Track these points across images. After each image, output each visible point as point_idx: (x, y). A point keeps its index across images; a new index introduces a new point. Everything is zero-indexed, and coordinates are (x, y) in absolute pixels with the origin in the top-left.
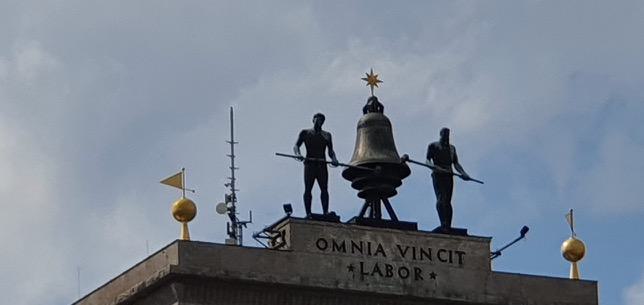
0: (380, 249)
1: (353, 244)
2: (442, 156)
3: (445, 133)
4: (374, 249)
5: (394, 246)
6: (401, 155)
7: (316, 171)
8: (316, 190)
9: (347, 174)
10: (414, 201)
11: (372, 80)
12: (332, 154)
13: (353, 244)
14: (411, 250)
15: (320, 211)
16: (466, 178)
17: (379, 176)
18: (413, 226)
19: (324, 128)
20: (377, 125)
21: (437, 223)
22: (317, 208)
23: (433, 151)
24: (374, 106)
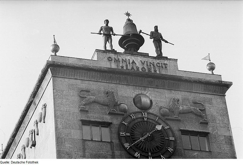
0: (133, 62)
1: (122, 59)
3: (156, 28)
4: (131, 62)
5: (139, 61)
6: (138, 30)
8: (108, 45)
12: (112, 32)
13: (122, 59)
14: (146, 62)
15: (110, 49)
16: (166, 42)
18: (146, 55)
19: (109, 25)
20: (130, 24)
21: (155, 55)
22: (109, 48)
24: (129, 20)
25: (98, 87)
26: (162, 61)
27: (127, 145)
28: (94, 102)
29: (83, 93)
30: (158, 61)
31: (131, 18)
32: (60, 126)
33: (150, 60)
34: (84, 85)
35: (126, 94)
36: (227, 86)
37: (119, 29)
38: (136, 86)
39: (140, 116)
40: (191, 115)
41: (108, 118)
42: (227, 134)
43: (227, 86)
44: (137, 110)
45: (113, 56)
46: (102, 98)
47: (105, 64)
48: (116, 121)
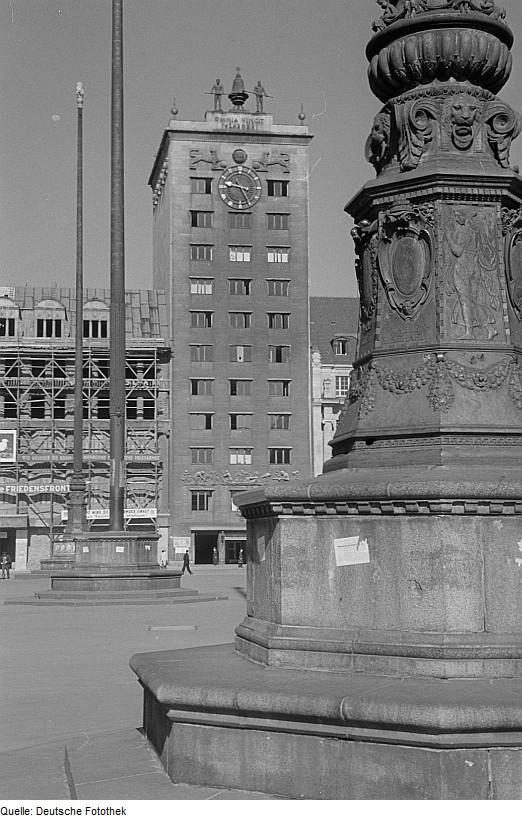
0: (236, 121)
3: (259, 83)
9: (230, 97)
10: (250, 103)
11: (238, 69)
17: (238, 99)
24: (238, 76)
25: (204, 145)
27: (224, 196)
30: (256, 117)
31: (240, 73)
33: (250, 117)
34: (194, 145)
35: (226, 149)
37: (228, 90)
39: (235, 169)
41: (210, 174)
44: (235, 164)
45: (219, 115)
46: (208, 156)
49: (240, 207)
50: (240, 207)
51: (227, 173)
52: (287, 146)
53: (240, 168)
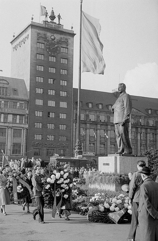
2: (59, 17)
7: (46, 16)
10: (56, 20)
17: (53, 17)
22: (46, 20)
23: (58, 16)
25: (42, 32)
26: (60, 26)
27: (48, 50)
28: (41, 37)
29: (38, 34)
32: (32, 43)
34: (39, 31)
35: (49, 34)
36: (75, 34)
38: (52, 33)
40: (65, 42)
41: (43, 42)
42: (73, 49)
43: (75, 34)
44: (51, 40)
45: (47, 23)
47: (44, 26)
48: (46, 43)
49: (53, 54)
50: (53, 54)
51: (49, 43)
52: (68, 37)
53: (53, 42)
